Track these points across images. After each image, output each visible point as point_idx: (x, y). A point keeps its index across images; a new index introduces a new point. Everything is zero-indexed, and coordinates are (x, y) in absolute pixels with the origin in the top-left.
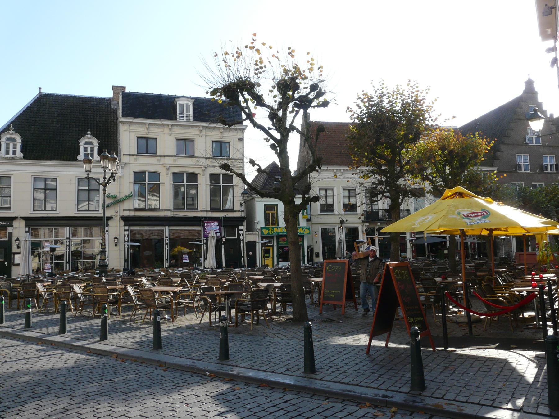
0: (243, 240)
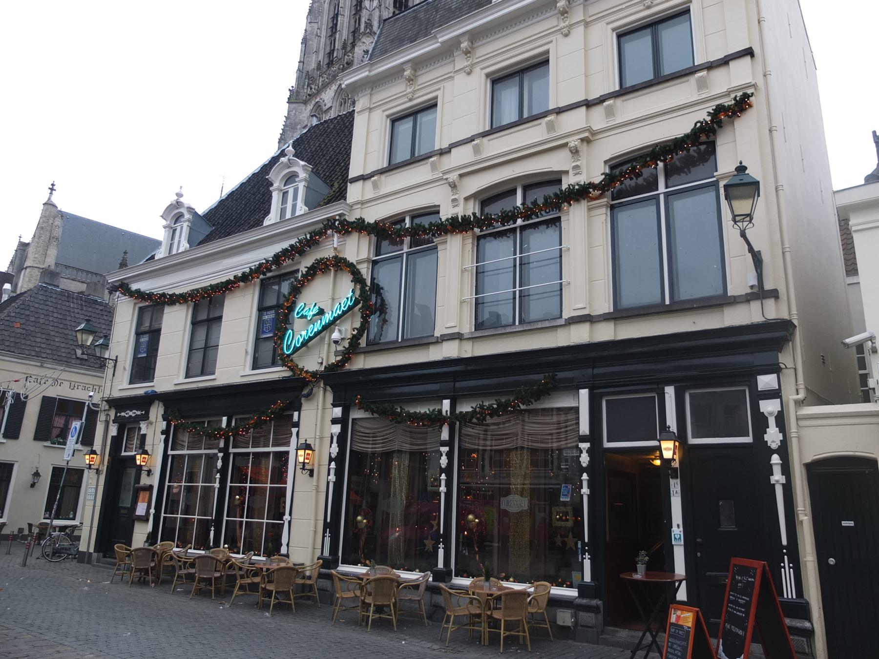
0: (784, 450)
